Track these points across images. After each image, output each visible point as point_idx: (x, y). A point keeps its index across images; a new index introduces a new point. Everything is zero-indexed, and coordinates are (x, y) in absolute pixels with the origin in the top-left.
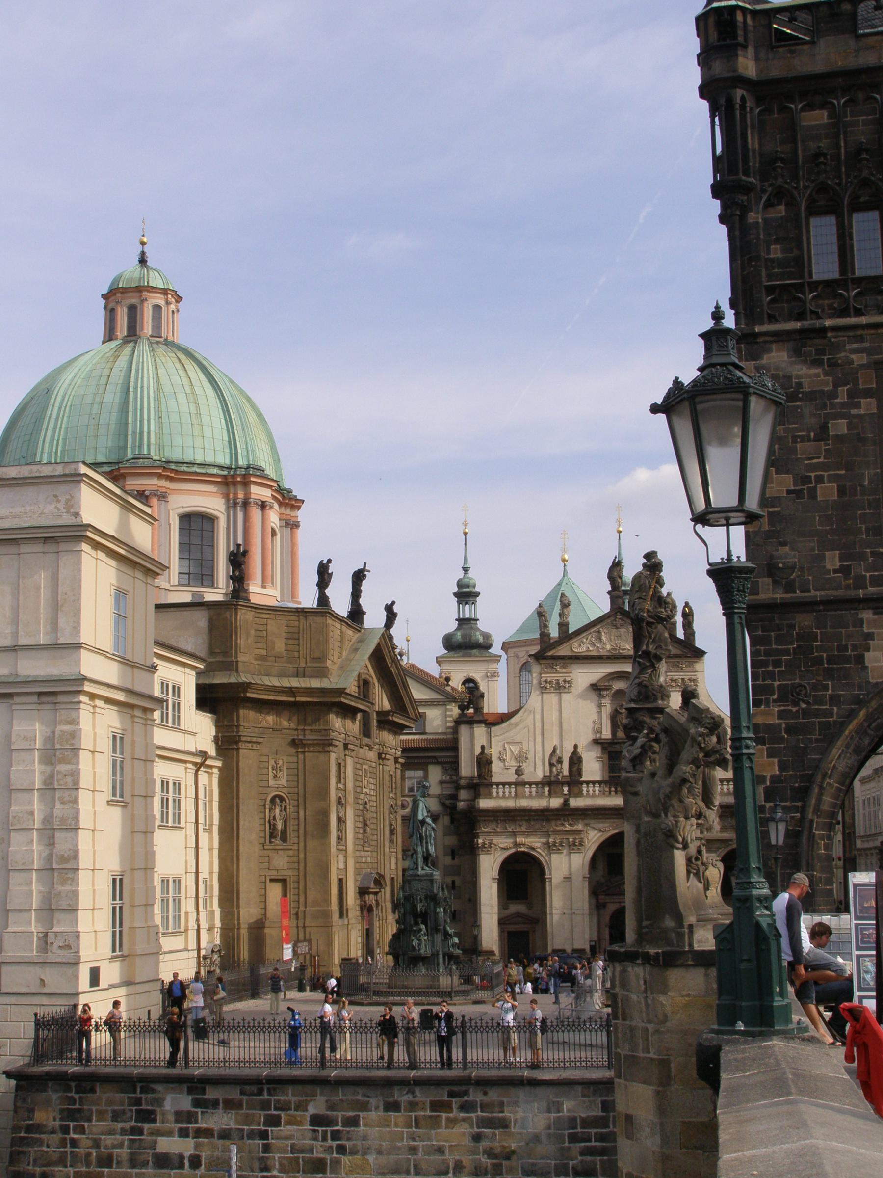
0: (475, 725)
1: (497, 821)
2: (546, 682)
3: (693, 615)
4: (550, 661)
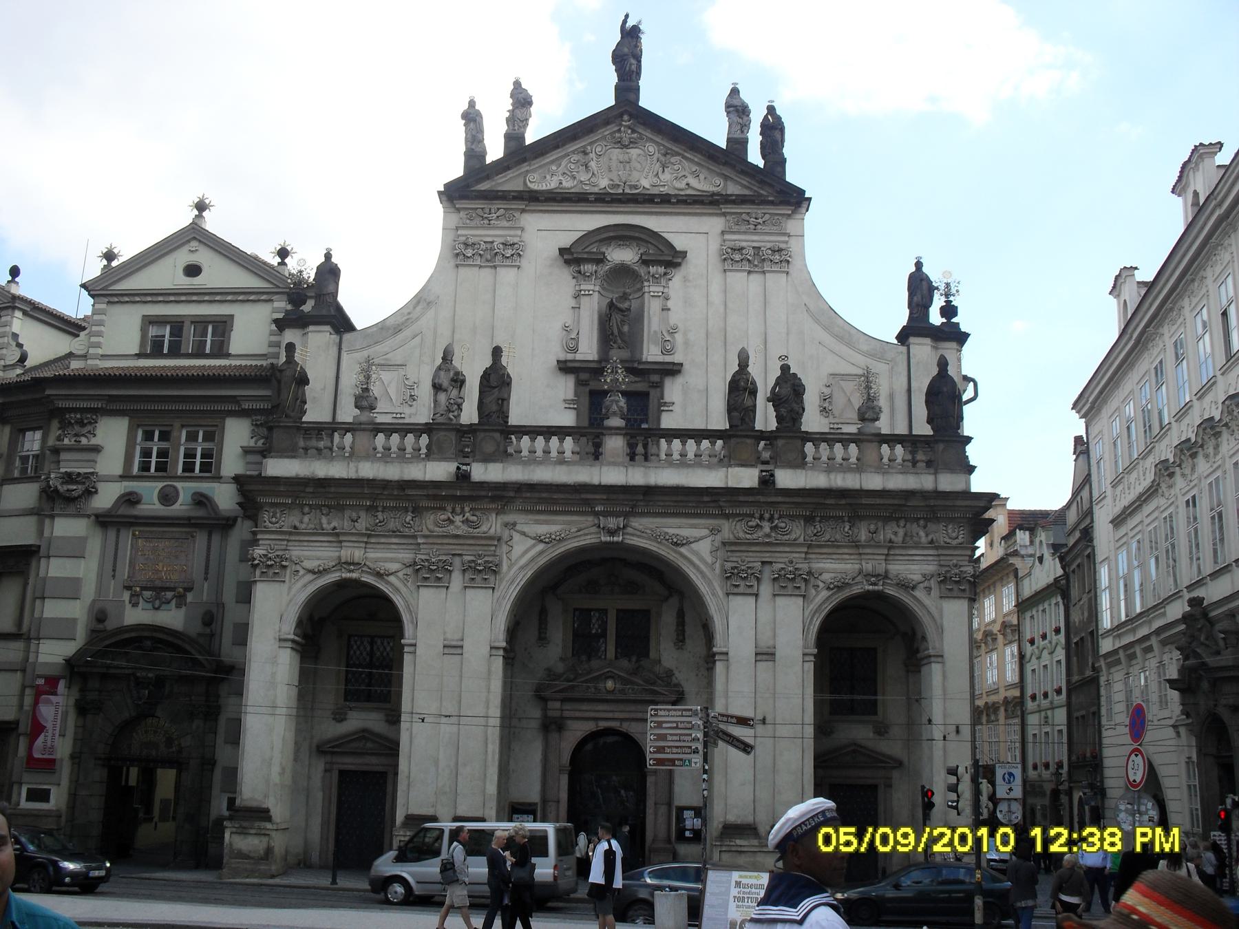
0: (311, 328)
1: (302, 506)
2: (466, 245)
3: (782, 130)
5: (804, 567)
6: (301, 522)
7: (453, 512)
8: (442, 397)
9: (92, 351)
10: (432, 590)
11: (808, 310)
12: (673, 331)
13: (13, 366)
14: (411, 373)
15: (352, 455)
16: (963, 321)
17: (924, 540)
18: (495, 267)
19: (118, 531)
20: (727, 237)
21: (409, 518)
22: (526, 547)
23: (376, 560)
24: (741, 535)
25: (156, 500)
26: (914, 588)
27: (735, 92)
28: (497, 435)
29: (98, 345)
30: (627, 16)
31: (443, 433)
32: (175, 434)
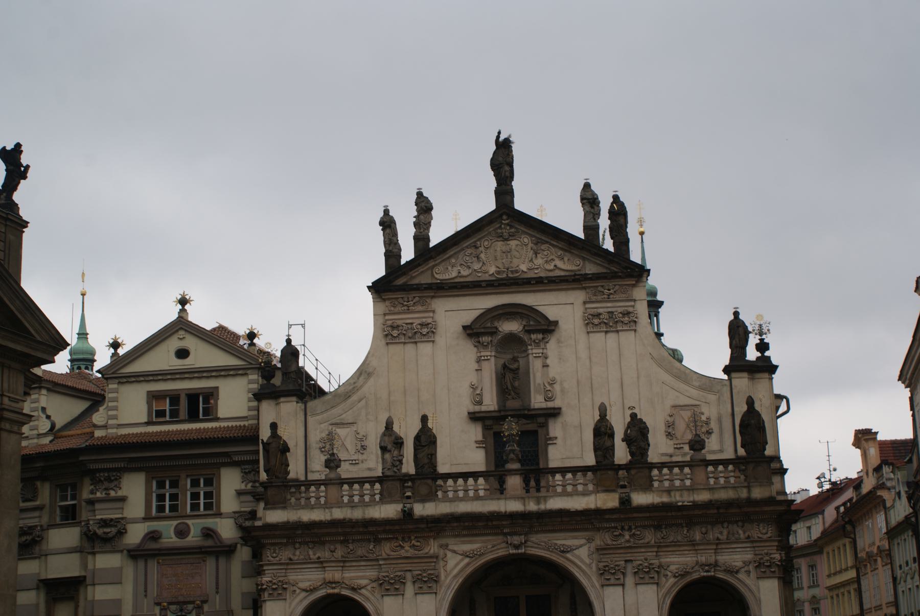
0: (282, 399)
1: (294, 543)
2: (393, 327)
4: (398, 295)
5: (656, 562)
6: (294, 555)
7: (403, 540)
8: (387, 456)
9: (110, 422)
10: (392, 598)
11: (653, 358)
12: (552, 383)
13: (45, 435)
14: (362, 428)
15: (326, 502)
16: (773, 354)
17: (742, 536)
18: (416, 343)
19: (146, 561)
20: (588, 306)
21: (371, 547)
22: (456, 561)
23: (351, 579)
24: (609, 542)
25: (173, 535)
26: (737, 572)
27: (587, 186)
28: (429, 481)
29: (115, 417)
30: (499, 133)
31: (391, 482)
32: (181, 483)
